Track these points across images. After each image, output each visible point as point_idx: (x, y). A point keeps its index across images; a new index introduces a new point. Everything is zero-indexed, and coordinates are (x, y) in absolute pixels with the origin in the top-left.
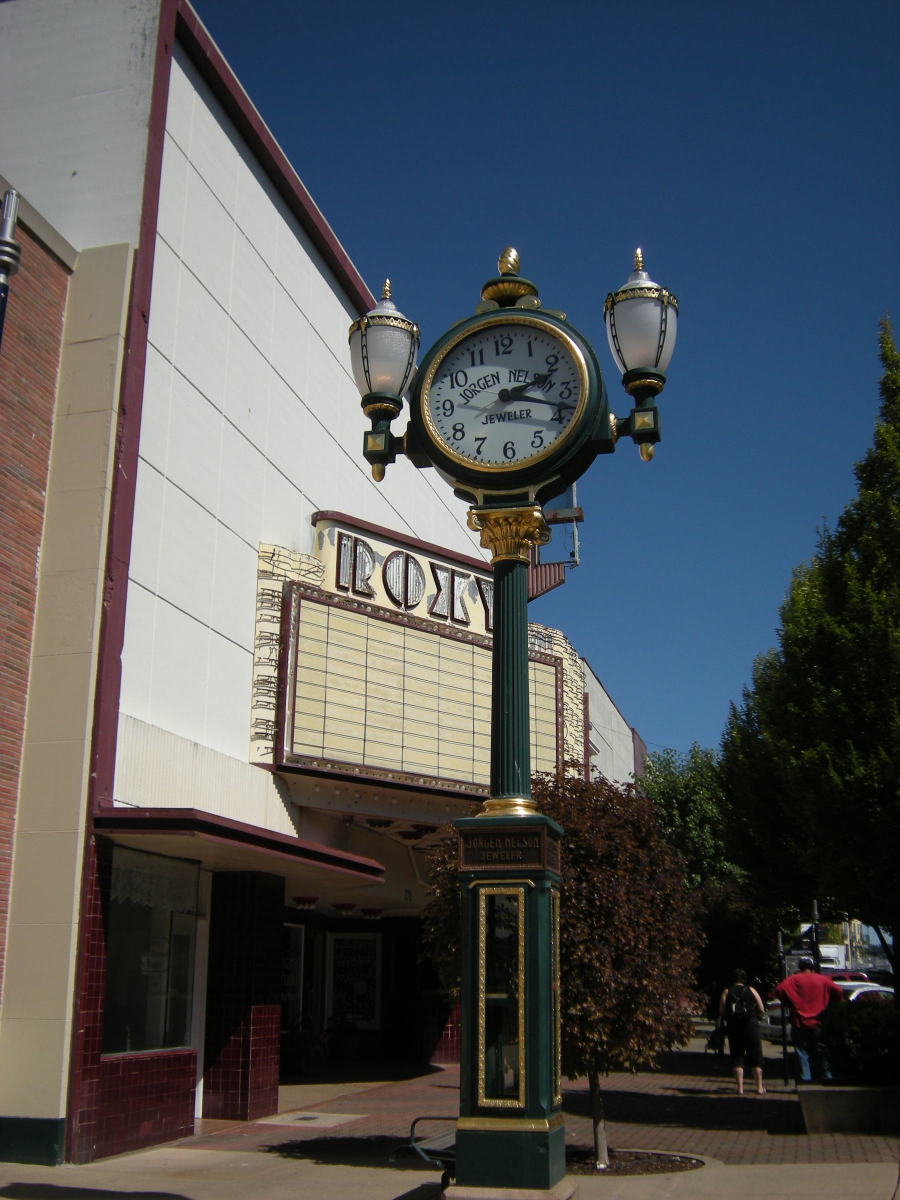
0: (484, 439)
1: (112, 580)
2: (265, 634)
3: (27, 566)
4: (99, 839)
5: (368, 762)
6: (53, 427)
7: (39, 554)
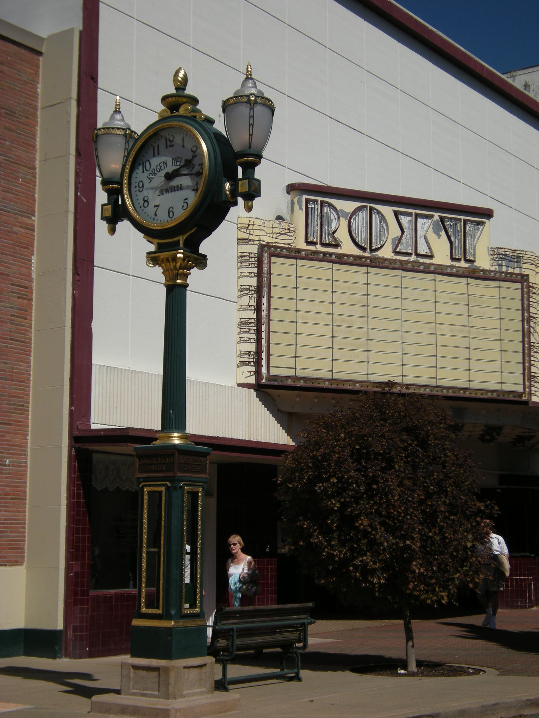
0: (158, 206)
1: (78, 275)
2: (244, 287)
3: (24, 270)
4: (78, 450)
5: (336, 376)
6: (37, 170)
7: (33, 261)
